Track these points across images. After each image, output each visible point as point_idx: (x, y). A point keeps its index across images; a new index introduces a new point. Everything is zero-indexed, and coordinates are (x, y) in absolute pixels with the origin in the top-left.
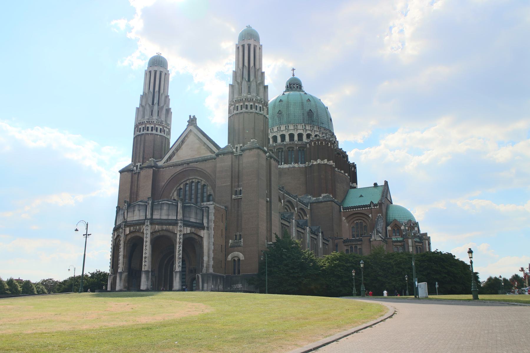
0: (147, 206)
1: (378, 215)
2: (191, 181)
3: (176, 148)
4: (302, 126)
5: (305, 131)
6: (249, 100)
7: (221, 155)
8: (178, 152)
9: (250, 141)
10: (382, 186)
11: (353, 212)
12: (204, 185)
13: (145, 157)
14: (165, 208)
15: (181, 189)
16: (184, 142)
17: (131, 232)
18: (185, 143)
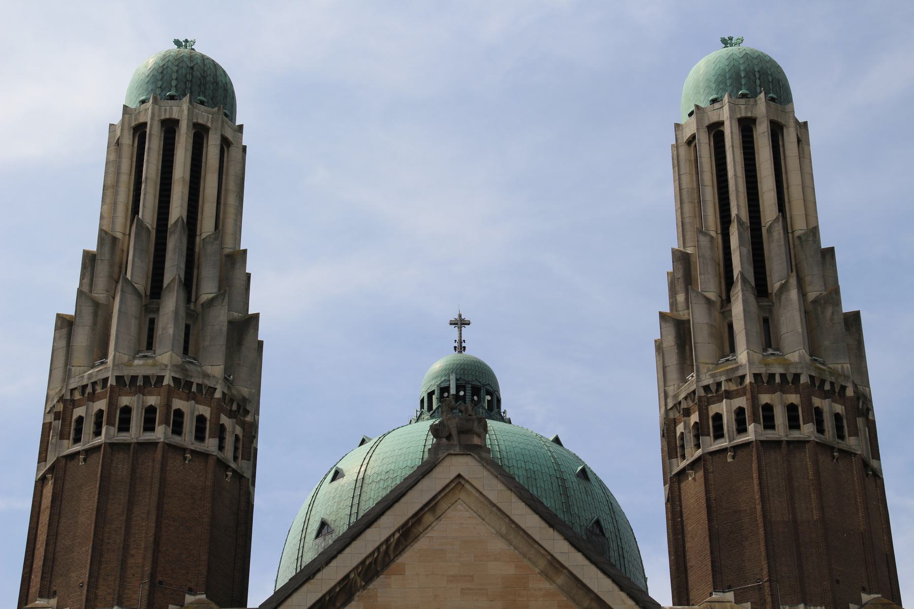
3: (363, 562)
6: (827, 387)
8: (371, 586)
13: (160, 578)
16: (416, 538)
18: (422, 544)
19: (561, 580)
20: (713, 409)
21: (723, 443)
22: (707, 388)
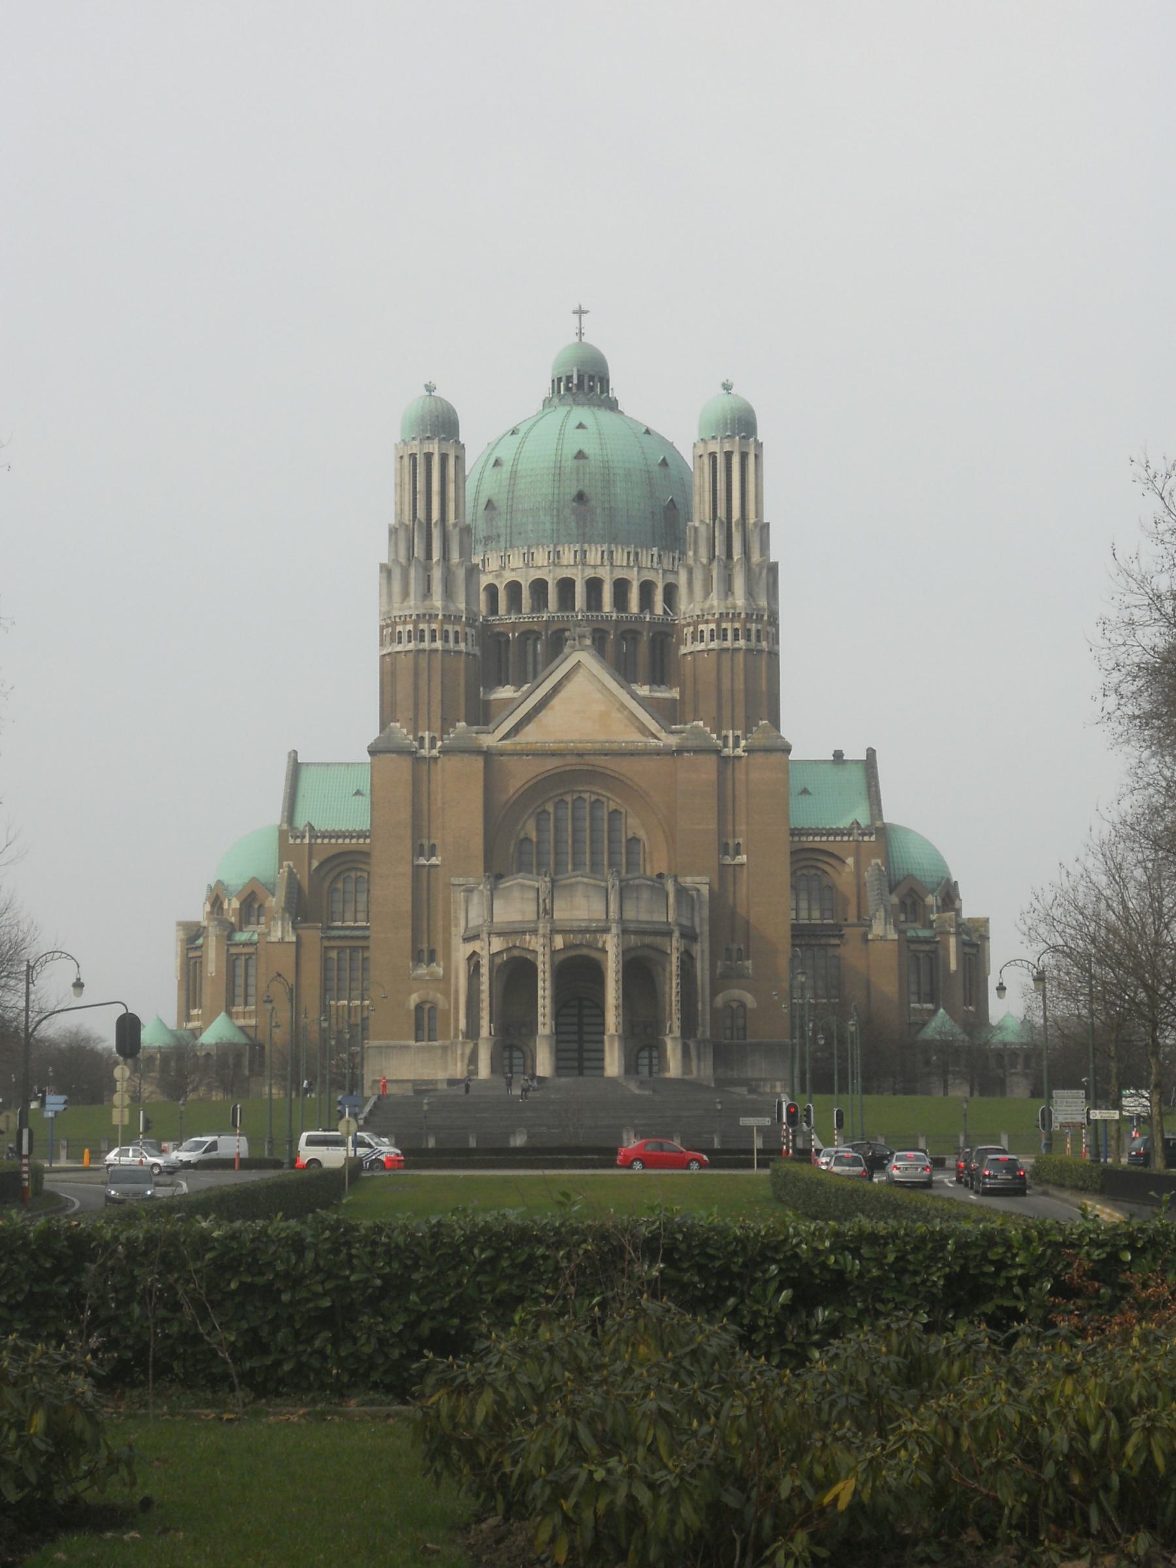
0: (607, 890)
1: (873, 861)
2: (575, 796)
4: (652, 555)
5: (661, 575)
6: (754, 617)
7: (688, 751)
9: (757, 725)
10: (857, 762)
11: (799, 846)
12: (616, 811)
14: (645, 895)
15: (545, 811)
17: (567, 947)
19: (626, 713)
20: (701, 627)
21: (702, 646)
22: (698, 616)
